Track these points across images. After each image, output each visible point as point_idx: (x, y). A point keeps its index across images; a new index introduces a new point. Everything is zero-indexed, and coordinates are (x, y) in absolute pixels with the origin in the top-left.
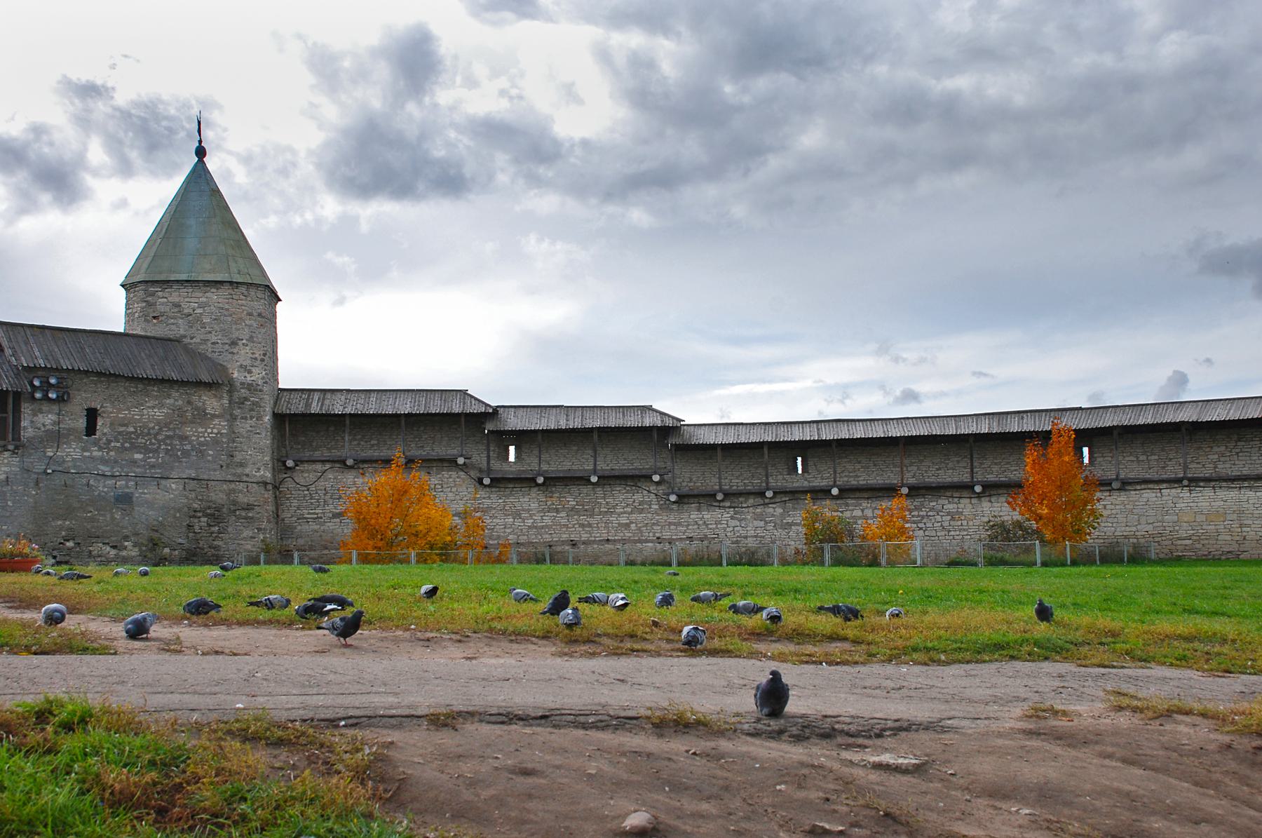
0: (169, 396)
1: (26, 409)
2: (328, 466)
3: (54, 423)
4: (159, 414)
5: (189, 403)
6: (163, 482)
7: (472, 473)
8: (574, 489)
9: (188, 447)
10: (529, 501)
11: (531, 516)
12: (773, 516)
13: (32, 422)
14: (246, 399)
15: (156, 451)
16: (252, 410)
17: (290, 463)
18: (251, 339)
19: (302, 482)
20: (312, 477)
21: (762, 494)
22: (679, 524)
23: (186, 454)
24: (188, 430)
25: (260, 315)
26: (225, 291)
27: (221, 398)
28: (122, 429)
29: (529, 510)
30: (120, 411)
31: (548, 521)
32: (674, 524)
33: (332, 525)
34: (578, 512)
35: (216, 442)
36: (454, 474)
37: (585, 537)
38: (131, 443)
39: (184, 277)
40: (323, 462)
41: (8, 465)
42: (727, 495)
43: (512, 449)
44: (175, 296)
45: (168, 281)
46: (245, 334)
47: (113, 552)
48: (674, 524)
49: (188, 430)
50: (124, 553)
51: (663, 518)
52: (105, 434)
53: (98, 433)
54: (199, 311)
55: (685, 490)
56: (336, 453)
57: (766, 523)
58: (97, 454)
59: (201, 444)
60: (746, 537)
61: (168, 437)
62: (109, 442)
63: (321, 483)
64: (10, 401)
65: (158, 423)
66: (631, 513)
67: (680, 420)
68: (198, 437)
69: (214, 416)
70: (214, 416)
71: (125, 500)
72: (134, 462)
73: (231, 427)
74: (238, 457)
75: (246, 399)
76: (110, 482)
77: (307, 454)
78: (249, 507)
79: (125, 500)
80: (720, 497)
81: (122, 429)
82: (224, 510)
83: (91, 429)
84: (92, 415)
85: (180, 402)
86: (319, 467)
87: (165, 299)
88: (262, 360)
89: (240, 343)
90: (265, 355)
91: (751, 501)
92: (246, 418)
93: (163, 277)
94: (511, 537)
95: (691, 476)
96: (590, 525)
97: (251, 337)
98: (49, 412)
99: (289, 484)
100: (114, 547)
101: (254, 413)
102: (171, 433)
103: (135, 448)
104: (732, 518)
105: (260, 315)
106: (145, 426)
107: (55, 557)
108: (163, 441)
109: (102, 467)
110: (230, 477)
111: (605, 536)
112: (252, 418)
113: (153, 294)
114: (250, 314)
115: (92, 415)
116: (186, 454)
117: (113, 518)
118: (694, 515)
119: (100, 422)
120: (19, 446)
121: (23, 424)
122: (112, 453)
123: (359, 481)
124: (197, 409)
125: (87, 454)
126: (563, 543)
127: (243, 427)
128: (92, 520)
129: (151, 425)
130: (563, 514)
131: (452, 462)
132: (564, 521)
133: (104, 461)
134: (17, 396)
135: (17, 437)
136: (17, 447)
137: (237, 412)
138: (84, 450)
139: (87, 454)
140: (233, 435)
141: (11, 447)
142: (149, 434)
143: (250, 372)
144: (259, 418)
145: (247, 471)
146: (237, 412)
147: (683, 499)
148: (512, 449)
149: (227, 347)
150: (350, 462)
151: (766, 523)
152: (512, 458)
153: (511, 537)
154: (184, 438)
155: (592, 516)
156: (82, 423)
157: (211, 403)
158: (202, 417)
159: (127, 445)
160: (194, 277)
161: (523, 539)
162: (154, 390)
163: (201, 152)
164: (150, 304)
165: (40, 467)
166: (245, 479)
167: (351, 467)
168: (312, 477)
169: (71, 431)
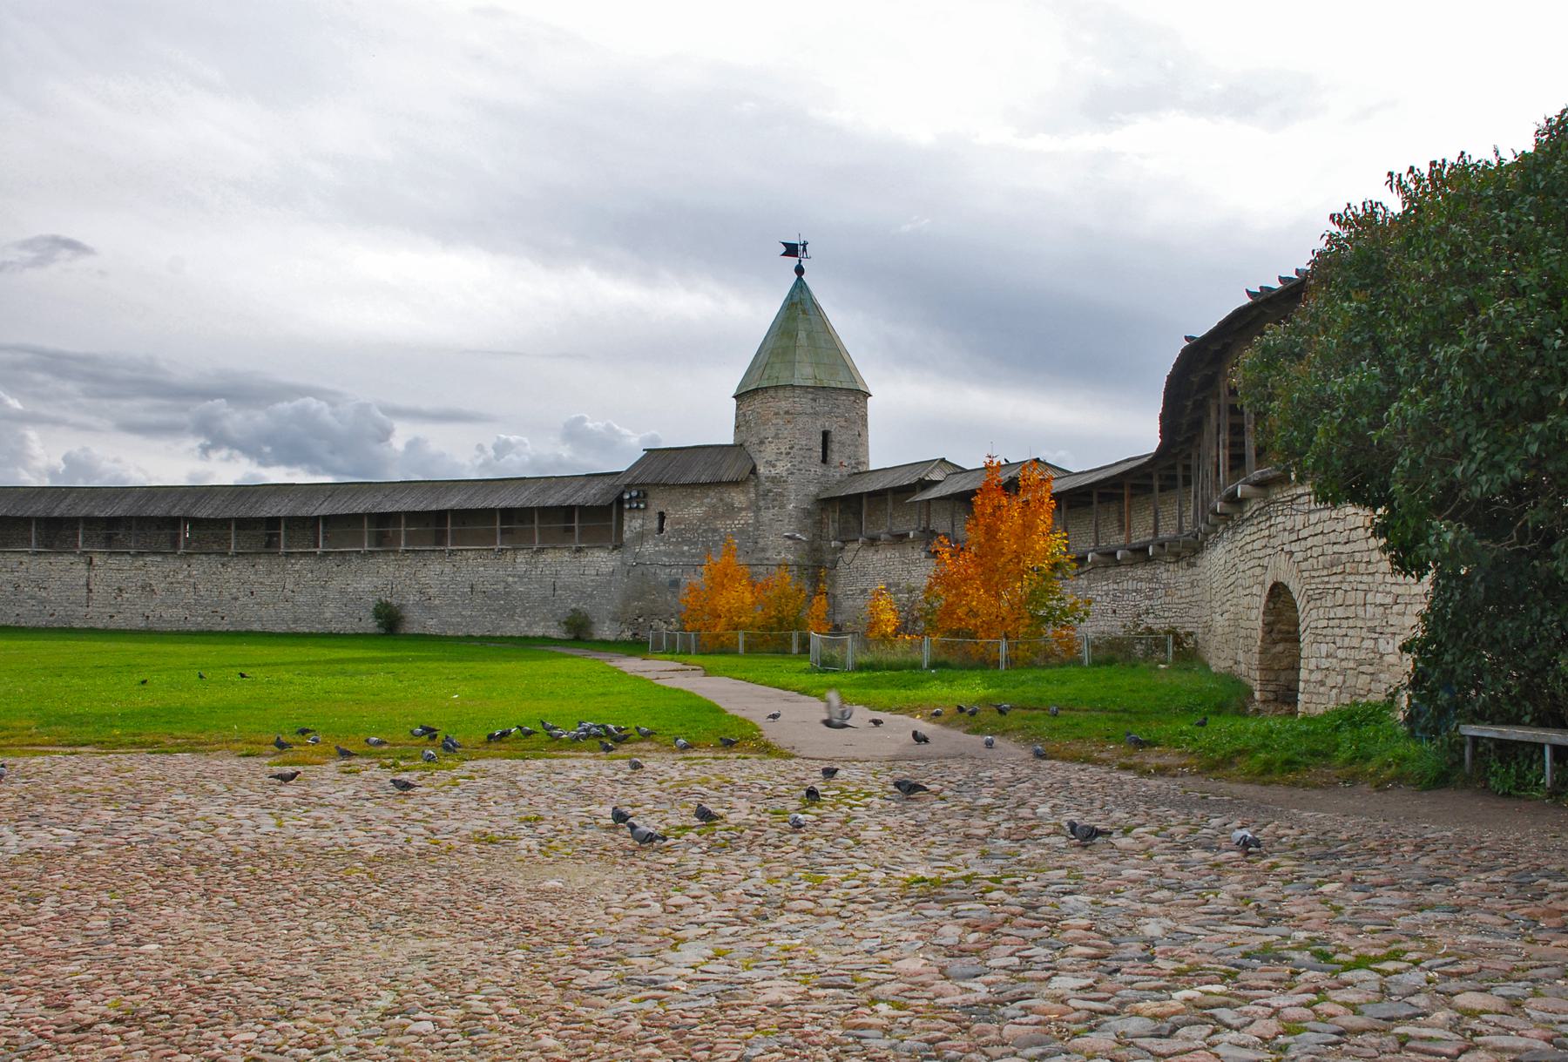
4: (699, 511)
15: (696, 543)
18: (776, 436)
20: (851, 555)
23: (715, 543)
24: (719, 524)
25: (787, 413)
35: (741, 531)
46: (771, 432)
49: (719, 524)
69: (741, 509)
70: (741, 509)
71: (675, 584)
72: (683, 553)
73: (756, 516)
74: (761, 543)
79: (675, 584)
83: (661, 529)
84: (662, 517)
99: (841, 563)
103: (685, 542)
105: (787, 413)
115: (662, 517)
120: (619, 546)
127: (766, 516)
128: (654, 601)
133: (666, 554)
137: (761, 503)
140: (758, 523)
144: (782, 507)
145: (768, 555)
154: (716, 530)
156: (656, 524)
157: (738, 498)
158: (731, 511)
163: (800, 270)
165: (631, 561)
168: (851, 555)
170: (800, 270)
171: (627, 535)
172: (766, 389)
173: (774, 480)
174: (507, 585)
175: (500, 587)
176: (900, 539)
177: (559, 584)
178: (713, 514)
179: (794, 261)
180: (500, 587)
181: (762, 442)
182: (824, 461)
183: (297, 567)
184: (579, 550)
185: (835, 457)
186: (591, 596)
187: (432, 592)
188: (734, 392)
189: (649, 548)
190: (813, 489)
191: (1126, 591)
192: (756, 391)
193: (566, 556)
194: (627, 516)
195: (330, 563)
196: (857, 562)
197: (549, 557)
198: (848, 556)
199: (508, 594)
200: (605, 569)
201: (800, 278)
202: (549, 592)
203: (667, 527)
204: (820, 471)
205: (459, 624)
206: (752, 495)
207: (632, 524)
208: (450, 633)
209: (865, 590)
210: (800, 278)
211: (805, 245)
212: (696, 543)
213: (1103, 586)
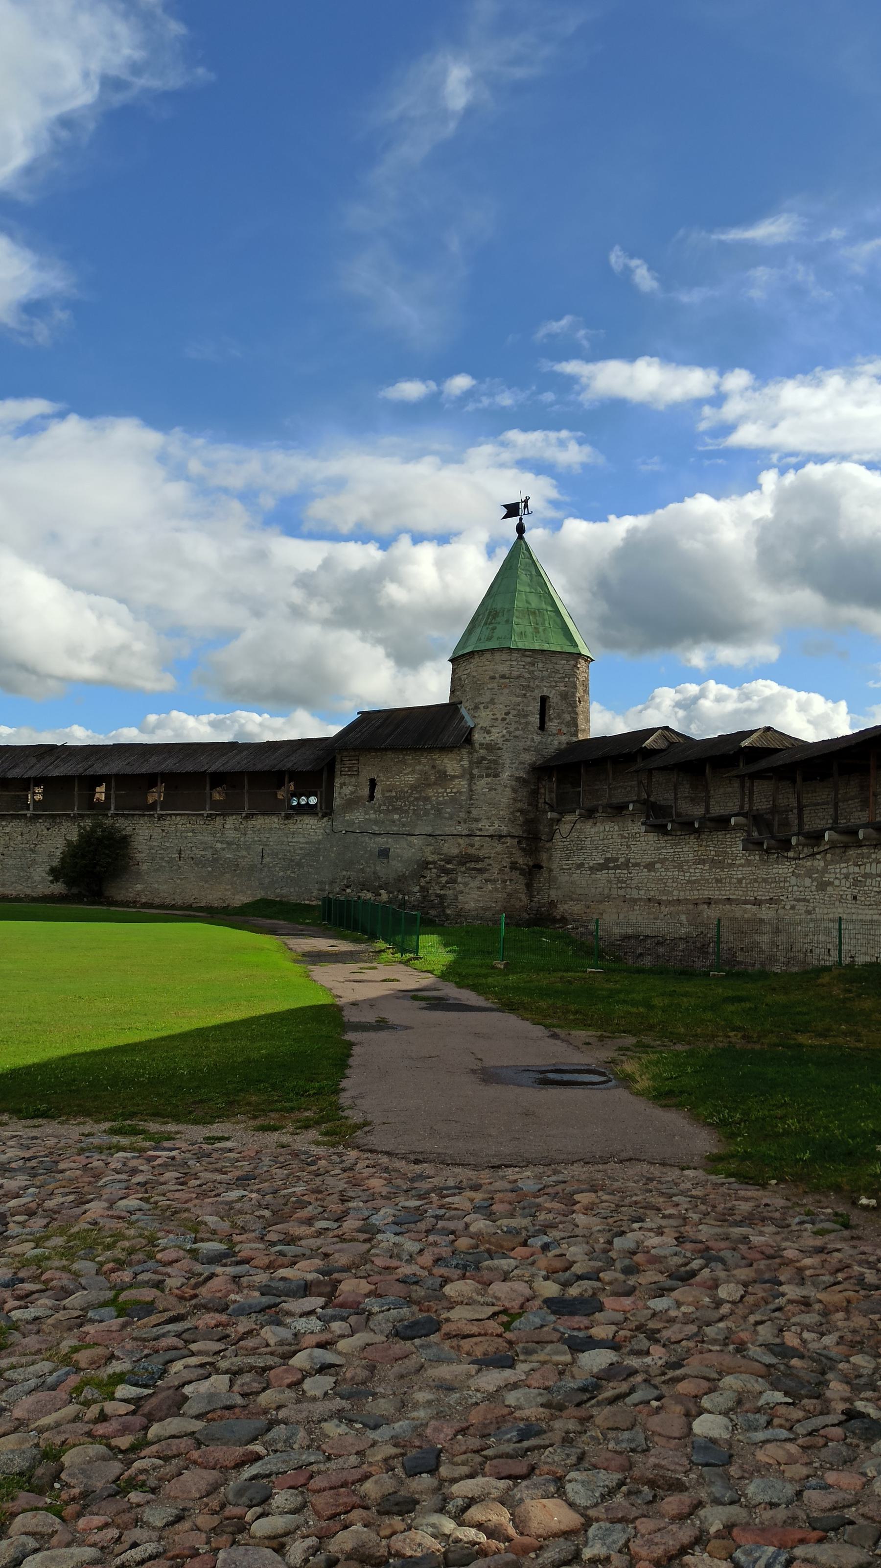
0: (420, 763)
3: (352, 793)
4: (411, 779)
5: (434, 767)
6: (409, 838)
9: (429, 807)
14: (484, 758)
15: (407, 812)
18: (492, 702)
20: (568, 827)
25: (503, 677)
28: (388, 794)
29: (688, 861)
30: (388, 778)
35: (453, 800)
49: (430, 792)
58: (373, 816)
59: (439, 803)
60: (799, 900)
61: (416, 799)
62: (380, 805)
68: (438, 797)
69: (454, 777)
71: (384, 853)
73: (470, 785)
74: (475, 813)
76: (379, 839)
79: (384, 853)
81: (388, 794)
83: (371, 797)
84: (373, 783)
88: (504, 719)
89: (481, 706)
90: (507, 714)
92: (482, 777)
97: (492, 700)
98: (350, 784)
99: (557, 836)
103: (395, 810)
106: (402, 791)
110: (466, 832)
112: (488, 776)
114: (493, 678)
115: (373, 783)
116: (427, 813)
121: (335, 795)
124: (439, 772)
137: (475, 771)
143: (489, 732)
145: (480, 826)
154: (427, 799)
156: (366, 792)
157: (451, 764)
163: (520, 529)
166: (478, 833)
170: (520, 529)
171: (337, 802)
172: (482, 652)
173: (491, 747)
174: (216, 851)
175: (208, 854)
176: (618, 811)
178: (425, 783)
179: (515, 521)
180: (208, 854)
181: (476, 708)
182: (542, 727)
183: (8, 830)
184: (288, 817)
185: (552, 725)
186: (299, 865)
188: (450, 655)
189: (358, 816)
190: (528, 758)
191: (866, 876)
192: (472, 653)
193: (274, 822)
194: (338, 781)
195: (41, 826)
196: (574, 834)
197: (259, 822)
198: (565, 828)
199: (215, 860)
200: (315, 838)
201: (521, 537)
203: (378, 794)
204: (537, 738)
206: (465, 763)
209: (583, 864)
210: (521, 537)
211: (526, 502)
213: (842, 868)
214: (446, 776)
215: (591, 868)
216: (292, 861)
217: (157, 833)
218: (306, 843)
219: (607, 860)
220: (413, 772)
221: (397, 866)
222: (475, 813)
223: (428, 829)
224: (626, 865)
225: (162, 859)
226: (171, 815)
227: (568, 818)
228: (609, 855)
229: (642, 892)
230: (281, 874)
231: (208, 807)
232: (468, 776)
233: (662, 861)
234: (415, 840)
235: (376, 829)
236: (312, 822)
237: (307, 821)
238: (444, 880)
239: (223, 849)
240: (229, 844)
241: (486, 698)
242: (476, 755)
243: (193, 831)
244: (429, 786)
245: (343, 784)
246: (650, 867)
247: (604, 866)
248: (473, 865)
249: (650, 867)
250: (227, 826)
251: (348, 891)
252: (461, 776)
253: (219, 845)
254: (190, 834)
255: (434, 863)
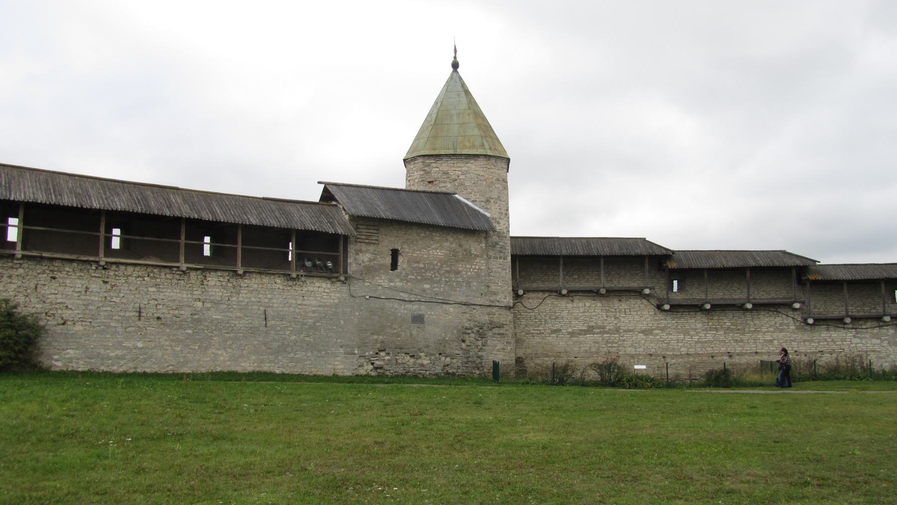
1: (352, 249)
2: (547, 294)
3: (370, 260)
4: (440, 253)
5: (460, 245)
6: (444, 306)
7: (652, 301)
8: (730, 314)
9: (460, 279)
10: (695, 322)
11: (697, 333)
12: (887, 335)
13: (355, 259)
16: (500, 252)
17: (521, 292)
19: (528, 306)
21: (878, 318)
22: (811, 341)
26: (481, 162)
27: (481, 242)
28: (415, 265)
29: (695, 329)
31: (709, 337)
32: (808, 341)
33: (552, 339)
34: (732, 331)
36: (639, 302)
37: (738, 350)
38: (422, 276)
39: (451, 152)
40: (544, 291)
41: (340, 291)
42: (855, 319)
43: (675, 282)
44: (444, 165)
45: (440, 155)
47: (412, 360)
48: (808, 341)
50: (419, 361)
51: (799, 336)
52: (404, 269)
53: (399, 268)
54: (462, 177)
55: (817, 316)
56: (554, 285)
57: (882, 341)
58: (399, 284)
61: (447, 272)
62: (407, 275)
63: (542, 307)
64: (341, 243)
65: (440, 261)
66: (774, 332)
67: (815, 261)
68: (467, 272)
69: (476, 256)
70: (476, 256)
71: (418, 319)
72: (424, 291)
74: (493, 287)
75: (497, 244)
76: (409, 306)
77: (527, 285)
78: (500, 326)
79: (418, 319)
80: (848, 320)
81: (415, 265)
82: (485, 328)
83: (394, 266)
84: (395, 254)
85: (454, 245)
86: (540, 295)
87: (437, 168)
89: (492, 201)
91: (869, 324)
92: (496, 258)
93: (436, 152)
94: (682, 349)
95: (823, 306)
96: (742, 341)
97: (499, 197)
98: (367, 251)
100: (412, 356)
101: (502, 255)
102: (448, 269)
103: (425, 280)
104: (854, 337)
107: (373, 364)
108: (443, 274)
109: (402, 294)
110: (488, 303)
111: (754, 350)
112: (500, 258)
113: (429, 165)
115: (395, 254)
117: (411, 335)
118: (824, 334)
119: (400, 259)
121: (350, 260)
122: (409, 284)
123: (570, 305)
124: (466, 250)
125: (392, 284)
126: (722, 354)
128: (398, 335)
129: (435, 262)
130: (721, 332)
131: (638, 293)
132: (722, 338)
134: (346, 238)
135: (345, 272)
136: (346, 279)
138: (390, 281)
139: (392, 284)
141: (342, 278)
142: (433, 269)
143: (499, 223)
146: (491, 253)
147: (820, 321)
148: (675, 282)
149: (483, 204)
150: (564, 292)
151: (882, 341)
152: (675, 289)
153: (682, 349)
154: (458, 273)
155: (743, 334)
156: (388, 260)
157: (475, 246)
158: (469, 257)
159: (419, 277)
160: (459, 152)
161: (692, 351)
162: (437, 236)
163: (455, 65)
164: (427, 173)
167: (564, 296)
169: (382, 266)
170: (455, 65)
171: (352, 268)
175: (186, 313)
177: (270, 313)
180: (186, 313)
181: (488, 201)
187: (67, 314)
199: (199, 321)
202: (258, 322)
205: (122, 357)
207: (359, 257)
208: (103, 368)
209: (559, 330)
212: (439, 282)
214: (471, 254)
215: (569, 333)
216: (304, 324)
217: (96, 286)
218: (319, 306)
219: (589, 326)
220: (442, 247)
221: (432, 332)
222: (493, 287)
223: (463, 299)
224: (617, 330)
225: (111, 317)
226: (117, 264)
227: (531, 295)
228: (592, 324)
229: (641, 350)
230: (293, 337)
231: (182, 258)
232: (485, 257)
233: (663, 329)
234: (451, 309)
235: (405, 296)
236: (324, 285)
237: (317, 284)
238: (480, 343)
239: (208, 309)
240: (216, 303)
241: (495, 195)
242: (490, 240)
243: (156, 285)
244: (457, 261)
245: (357, 252)
246: (646, 332)
247: (586, 332)
248: (496, 331)
249: (646, 332)
250: (212, 283)
251: (382, 354)
252: (481, 256)
253: (200, 304)
254: (154, 289)
255: (470, 329)
